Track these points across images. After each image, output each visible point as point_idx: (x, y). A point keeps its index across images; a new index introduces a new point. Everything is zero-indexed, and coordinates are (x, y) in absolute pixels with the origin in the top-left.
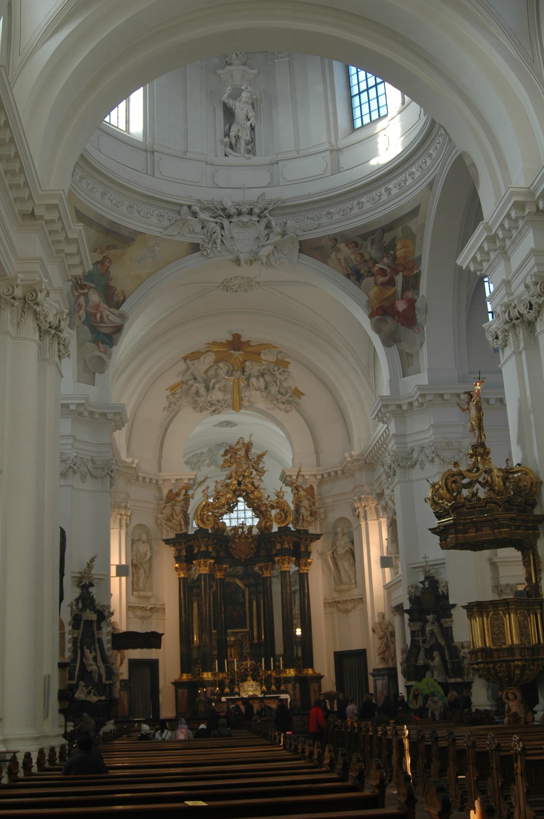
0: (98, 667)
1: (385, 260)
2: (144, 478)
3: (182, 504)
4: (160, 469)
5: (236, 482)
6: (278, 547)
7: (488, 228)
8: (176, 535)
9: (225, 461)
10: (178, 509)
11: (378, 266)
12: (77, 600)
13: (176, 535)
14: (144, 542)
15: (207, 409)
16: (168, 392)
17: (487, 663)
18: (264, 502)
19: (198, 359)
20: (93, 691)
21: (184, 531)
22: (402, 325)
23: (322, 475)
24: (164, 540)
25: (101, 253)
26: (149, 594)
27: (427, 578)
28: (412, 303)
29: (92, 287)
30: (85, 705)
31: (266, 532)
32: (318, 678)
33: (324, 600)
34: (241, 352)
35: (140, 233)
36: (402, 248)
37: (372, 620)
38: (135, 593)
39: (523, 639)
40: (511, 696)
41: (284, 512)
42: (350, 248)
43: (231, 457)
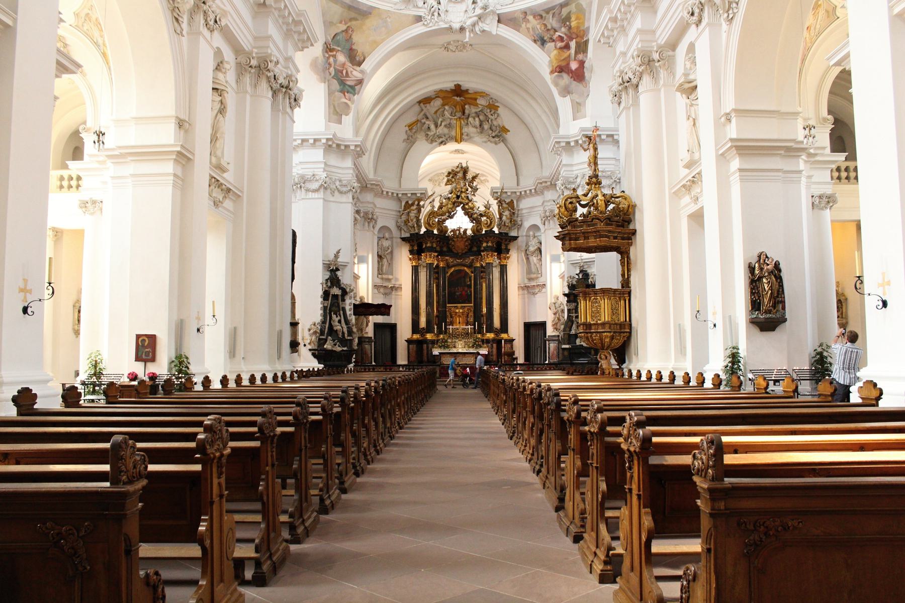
0: (342, 327)
1: (563, 29)
2: (387, 192)
3: (415, 212)
4: (400, 187)
5: (455, 196)
6: (484, 245)
7: (611, 12)
8: (411, 234)
9: (448, 181)
10: (412, 215)
11: (558, 34)
12: (327, 280)
13: (411, 234)
16: (407, 128)
17: (587, 333)
18: (475, 212)
19: (430, 103)
20: (338, 343)
21: (417, 231)
22: (574, 80)
23: (521, 193)
24: (401, 238)
25: (346, 24)
26: (390, 277)
27: (581, 271)
28: (582, 63)
29: (338, 50)
30: (332, 352)
31: (477, 234)
32: (511, 341)
33: (518, 284)
34: (462, 98)
35: (375, 8)
36: (576, 20)
37: (550, 300)
38: (380, 276)
39: (614, 317)
40: (603, 357)
42: (536, 20)
43: (452, 177)
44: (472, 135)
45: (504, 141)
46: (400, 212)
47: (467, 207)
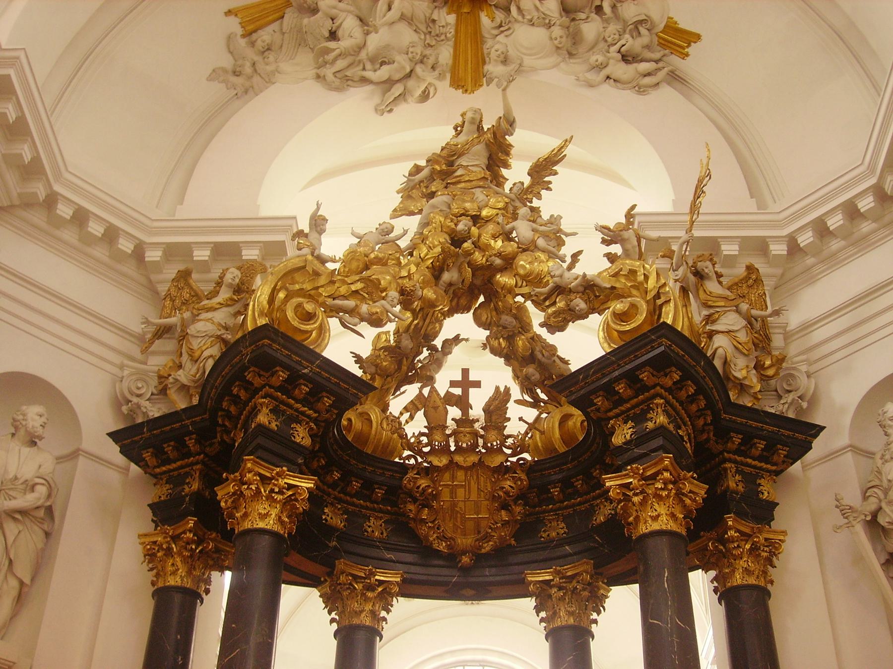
5: (444, 238)
6: (622, 434)
14: (32, 443)
15: (364, 80)
16: (234, 25)
41: (647, 302)
44: (528, 61)
45: (675, 78)
46: (140, 338)
47: (504, 279)
